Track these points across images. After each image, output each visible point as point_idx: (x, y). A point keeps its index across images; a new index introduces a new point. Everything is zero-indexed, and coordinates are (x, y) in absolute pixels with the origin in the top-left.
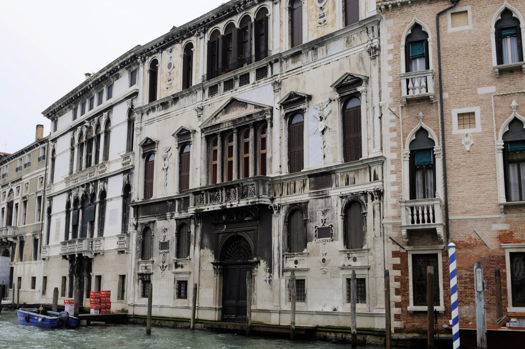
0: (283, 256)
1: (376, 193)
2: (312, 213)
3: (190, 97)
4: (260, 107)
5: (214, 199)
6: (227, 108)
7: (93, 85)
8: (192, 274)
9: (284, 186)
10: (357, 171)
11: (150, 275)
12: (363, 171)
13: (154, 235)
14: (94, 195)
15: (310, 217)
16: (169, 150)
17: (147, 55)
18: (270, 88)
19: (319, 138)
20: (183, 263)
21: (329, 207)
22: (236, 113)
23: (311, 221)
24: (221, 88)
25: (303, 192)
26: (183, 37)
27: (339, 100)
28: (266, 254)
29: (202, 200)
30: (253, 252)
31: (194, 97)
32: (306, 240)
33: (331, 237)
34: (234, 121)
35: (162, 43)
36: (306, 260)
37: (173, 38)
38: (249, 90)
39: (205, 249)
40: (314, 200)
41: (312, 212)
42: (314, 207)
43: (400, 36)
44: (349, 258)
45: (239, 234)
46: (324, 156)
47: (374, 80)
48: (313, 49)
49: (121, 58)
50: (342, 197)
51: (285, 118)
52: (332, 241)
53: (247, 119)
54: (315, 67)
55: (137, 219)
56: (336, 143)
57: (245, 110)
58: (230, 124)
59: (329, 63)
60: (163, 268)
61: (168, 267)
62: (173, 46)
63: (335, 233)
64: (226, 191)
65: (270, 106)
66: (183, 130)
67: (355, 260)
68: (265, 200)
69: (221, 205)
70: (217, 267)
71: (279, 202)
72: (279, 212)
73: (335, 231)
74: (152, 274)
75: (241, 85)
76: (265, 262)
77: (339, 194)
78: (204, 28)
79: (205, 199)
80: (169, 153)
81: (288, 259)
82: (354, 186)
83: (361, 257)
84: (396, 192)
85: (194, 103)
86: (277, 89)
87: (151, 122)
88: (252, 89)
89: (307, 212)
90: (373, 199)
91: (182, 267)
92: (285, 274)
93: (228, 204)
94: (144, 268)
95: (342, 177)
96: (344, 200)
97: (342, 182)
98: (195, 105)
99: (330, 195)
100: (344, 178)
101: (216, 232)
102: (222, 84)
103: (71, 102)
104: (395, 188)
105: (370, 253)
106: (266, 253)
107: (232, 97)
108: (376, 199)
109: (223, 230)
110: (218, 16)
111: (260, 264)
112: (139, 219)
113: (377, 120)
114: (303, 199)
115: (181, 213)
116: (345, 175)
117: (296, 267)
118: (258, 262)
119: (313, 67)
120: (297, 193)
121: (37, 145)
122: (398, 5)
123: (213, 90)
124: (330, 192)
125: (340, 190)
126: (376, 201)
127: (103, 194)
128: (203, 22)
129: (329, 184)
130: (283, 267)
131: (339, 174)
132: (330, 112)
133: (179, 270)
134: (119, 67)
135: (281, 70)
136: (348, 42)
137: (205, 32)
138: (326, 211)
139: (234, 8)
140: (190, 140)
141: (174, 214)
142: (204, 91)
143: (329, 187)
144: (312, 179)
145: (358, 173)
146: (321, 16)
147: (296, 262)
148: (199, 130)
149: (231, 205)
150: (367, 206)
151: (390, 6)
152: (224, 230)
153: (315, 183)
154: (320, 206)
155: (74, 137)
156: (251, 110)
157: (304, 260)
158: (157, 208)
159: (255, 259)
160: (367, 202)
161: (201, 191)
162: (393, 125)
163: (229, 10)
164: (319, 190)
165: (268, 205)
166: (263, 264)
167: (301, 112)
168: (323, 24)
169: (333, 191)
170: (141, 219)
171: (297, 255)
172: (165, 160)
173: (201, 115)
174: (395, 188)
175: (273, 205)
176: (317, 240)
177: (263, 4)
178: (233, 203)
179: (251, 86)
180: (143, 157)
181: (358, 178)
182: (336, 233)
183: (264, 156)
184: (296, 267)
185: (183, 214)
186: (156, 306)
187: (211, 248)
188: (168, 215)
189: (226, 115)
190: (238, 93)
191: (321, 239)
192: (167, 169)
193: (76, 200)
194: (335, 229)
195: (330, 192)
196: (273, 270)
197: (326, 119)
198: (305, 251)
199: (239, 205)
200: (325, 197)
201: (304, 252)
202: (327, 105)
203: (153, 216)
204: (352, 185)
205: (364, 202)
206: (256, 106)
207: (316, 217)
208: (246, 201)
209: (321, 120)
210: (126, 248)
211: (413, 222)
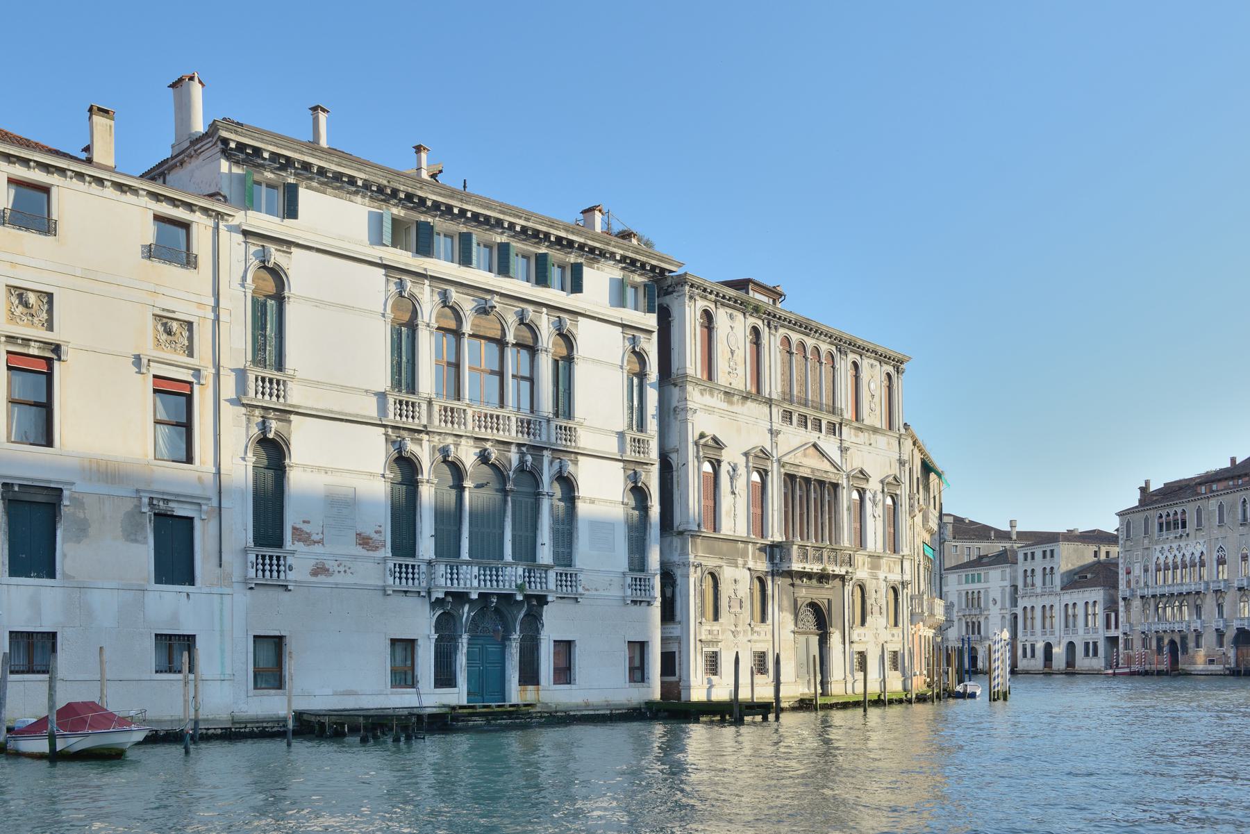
58: (809, 471)
128: (780, 317)
133: (755, 637)
188: (740, 561)
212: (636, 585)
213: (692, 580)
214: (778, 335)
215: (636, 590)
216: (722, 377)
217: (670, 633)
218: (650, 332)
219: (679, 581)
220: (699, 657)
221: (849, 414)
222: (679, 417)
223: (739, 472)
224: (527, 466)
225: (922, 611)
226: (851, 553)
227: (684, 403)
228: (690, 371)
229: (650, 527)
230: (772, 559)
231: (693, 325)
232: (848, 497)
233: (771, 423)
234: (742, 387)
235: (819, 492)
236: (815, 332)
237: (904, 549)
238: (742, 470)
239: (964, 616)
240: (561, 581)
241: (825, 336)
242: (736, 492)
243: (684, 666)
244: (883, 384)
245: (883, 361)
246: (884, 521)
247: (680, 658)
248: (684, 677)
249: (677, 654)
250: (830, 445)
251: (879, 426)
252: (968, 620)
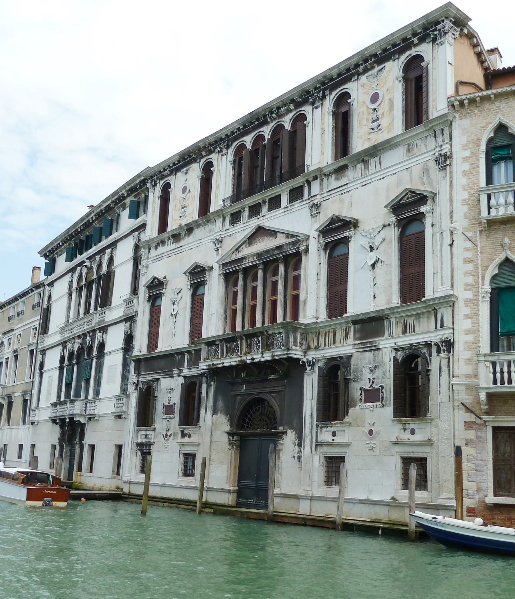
0: (317, 426)
1: (444, 344)
2: (356, 370)
4: (293, 236)
5: (231, 351)
6: (251, 239)
7: (96, 218)
8: (201, 446)
9: (320, 335)
10: (418, 316)
11: (150, 445)
12: (426, 316)
13: (157, 397)
14: (91, 348)
15: (354, 375)
16: (180, 292)
17: (158, 178)
18: (306, 212)
19: (368, 274)
20: (190, 432)
21: (379, 363)
23: (354, 381)
24: (245, 214)
25: (345, 342)
26: (201, 155)
27: (396, 224)
28: (295, 422)
29: (216, 352)
30: (278, 420)
31: (212, 226)
32: (348, 404)
33: (382, 402)
34: (259, 255)
35: (176, 162)
36: (347, 431)
37: (190, 156)
38: (280, 215)
39: (219, 414)
40: (359, 353)
41: (357, 369)
42: (359, 362)
43: (479, 140)
44: (405, 429)
45: (261, 396)
46: (374, 297)
47: (443, 199)
48: (363, 161)
49: (128, 183)
50: (397, 350)
51: (324, 249)
52: (383, 407)
53: (276, 252)
54: (364, 184)
55: (138, 376)
56: (391, 280)
57: (273, 240)
59: (384, 178)
61: (172, 436)
62: (190, 166)
63: (386, 397)
64: (247, 342)
65: (305, 235)
66: (197, 266)
67: (413, 432)
68: (297, 353)
69: (240, 359)
70: (233, 438)
71: (314, 356)
72: (313, 368)
73: (386, 394)
75: (270, 209)
76: (294, 433)
77: (393, 345)
78: (227, 143)
79: (220, 352)
80: (180, 295)
81: (324, 429)
82: (414, 335)
83: (421, 428)
84: (470, 343)
85: (212, 234)
86: (315, 214)
87: (159, 258)
88: (283, 214)
89: (350, 369)
90: (439, 352)
91: (190, 436)
92: (319, 448)
93: (249, 357)
94: (143, 436)
95: (397, 324)
96: (399, 353)
97: (397, 330)
98: (213, 237)
99: (381, 347)
100: (400, 325)
101: (233, 393)
102: (247, 210)
103: (71, 239)
104: (470, 338)
105: (434, 423)
106: (295, 422)
107: (258, 225)
108: (444, 352)
109: (241, 391)
110: (245, 126)
111: (286, 435)
112: (141, 377)
113: (446, 249)
114: (344, 352)
115: (191, 369)
116: (402, 321)
117: (333, 440)
118: (285, 433)
119: (362, 184)
120: (337, 345)
121: (32, 291)
122: (476, 101)
123: (236, 218)
124: (381, 343)
125: (393, 341)
126: (444, 354)
127: (102, 346)
129: (379, 332)
130: (317, 440)
131: (393, 320)
132: (384, 240)
133: (186, 440)
134: (125, 195)
135: (322, 189)
136: (409, 150)
137: (227, 148)
138: (375, 367)
139: (265, 116)
140: (206, 279)
141: (182, 370)
142: (224, 219)
143: (380, 337)
144: (358, 326)
145: (420, 317)
146: (374, 119)
147: (334, 434)
148: (216, 266)
149: (253, 359)
150: (431, 361)
151: (466, 102)
152: (243, 391)
153: (361, 331)
154: (367, 361)
155: (72, 280)
156: (281, 240)
157: (344, 431)
158: (162, 363)
159: (281, 429)
160: (430, 355)
161: (215, 341)
162: (469, 255)
163: (258, 119)
164: (366, 341)
165: (299, 360)
166: (291, 436)
167: (346, 241)
168: (376, 130)
169: (386, 342)
170: (143, 376)
171: (335, 424)
172: (174, 304)
173: (220, 249)
174: (470, 338)
175: (305, 360)
176: (362, 405)
177: (300, 109)
178: (255, 357)
179: (283, 211)
180: (149, 301)
181: (419, 324)
182: (388, 396)
183: (296, 299)
184: (333, 440)
185: (193, 370)
186: (155, 485)
187: (226, 414)
188: (175, 371)
189: (250, 247)
190: (266, 220)
191: (367, 404)
192: (176, 315)
193: (71, 354)
194: (386, 391)
195: (381, 343)
196: (304, 443)
197: (377, 249)
198: (347, 419)
199: (262, 359)
200: (375, 350)
201: (344, 421)
202: (379, 231)
203: (157, 373)
204: (411, 334)
205: (427, 355)
206: (288, 235)
207: (361, 375)
208: (270, 355)
209: (371, 251)
210: (124, 412)
211: (495, 382)
245: (394, 53)
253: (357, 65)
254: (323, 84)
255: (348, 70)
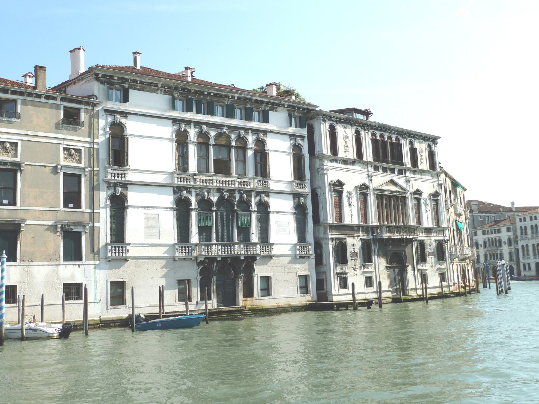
3: (362, 165)
5: (398, 232)
11: (346, 273)
22: (392, 188)
48: (421, 172)
60: (355, 269)
72: (415, 243)
74: (347, 273)
137: (369, 131)
139: (386, 129)
144: (425, 230)
159: (407, 264)
186: (358, 293)
206: (402, 188)
212: (301, 249)
213: (330, 246)
214: (369, 133)
215: (301, 251)
216: (342, 154)
217: (321, 270)
218: (302, 137)
219: (324, 246)
220: (336, 281)
221: (409, 165)
222: (320, 173)
223: (352, 195)
224: (244, 199)
225: (456, 253)
226: (415, 228)
227: (322, 166)
228: (325, 153)
229: (308, 223)
230: (373, 233)
231: (325, 132)
232: (410, 203)
233: (368, 172)
234: (352, 157)
235: (396, 201)
236: (389, 130)
237: (444, 224)
238: (354, 194)
239: (488, 251)
240: (263, 249)
241: (394, 131)
242: (352, 204)
243: (329, 285)
244: (426, 150)
246: (432, 212)
247: (326, 281)
248: (329, 290)
249: (325, 280)
250: (400, 180)
251: (425, 168)
252: (491, 253)
253: (417, 135)
254: (408, 133)
255: (415, 135)
